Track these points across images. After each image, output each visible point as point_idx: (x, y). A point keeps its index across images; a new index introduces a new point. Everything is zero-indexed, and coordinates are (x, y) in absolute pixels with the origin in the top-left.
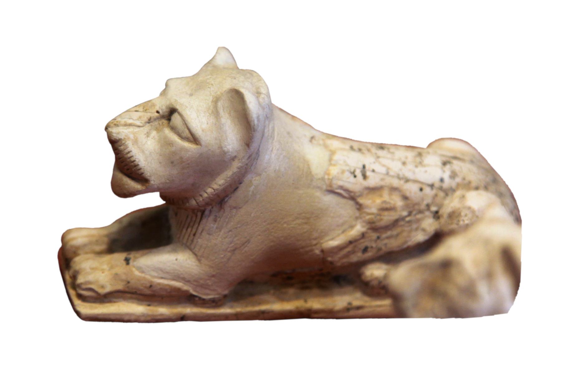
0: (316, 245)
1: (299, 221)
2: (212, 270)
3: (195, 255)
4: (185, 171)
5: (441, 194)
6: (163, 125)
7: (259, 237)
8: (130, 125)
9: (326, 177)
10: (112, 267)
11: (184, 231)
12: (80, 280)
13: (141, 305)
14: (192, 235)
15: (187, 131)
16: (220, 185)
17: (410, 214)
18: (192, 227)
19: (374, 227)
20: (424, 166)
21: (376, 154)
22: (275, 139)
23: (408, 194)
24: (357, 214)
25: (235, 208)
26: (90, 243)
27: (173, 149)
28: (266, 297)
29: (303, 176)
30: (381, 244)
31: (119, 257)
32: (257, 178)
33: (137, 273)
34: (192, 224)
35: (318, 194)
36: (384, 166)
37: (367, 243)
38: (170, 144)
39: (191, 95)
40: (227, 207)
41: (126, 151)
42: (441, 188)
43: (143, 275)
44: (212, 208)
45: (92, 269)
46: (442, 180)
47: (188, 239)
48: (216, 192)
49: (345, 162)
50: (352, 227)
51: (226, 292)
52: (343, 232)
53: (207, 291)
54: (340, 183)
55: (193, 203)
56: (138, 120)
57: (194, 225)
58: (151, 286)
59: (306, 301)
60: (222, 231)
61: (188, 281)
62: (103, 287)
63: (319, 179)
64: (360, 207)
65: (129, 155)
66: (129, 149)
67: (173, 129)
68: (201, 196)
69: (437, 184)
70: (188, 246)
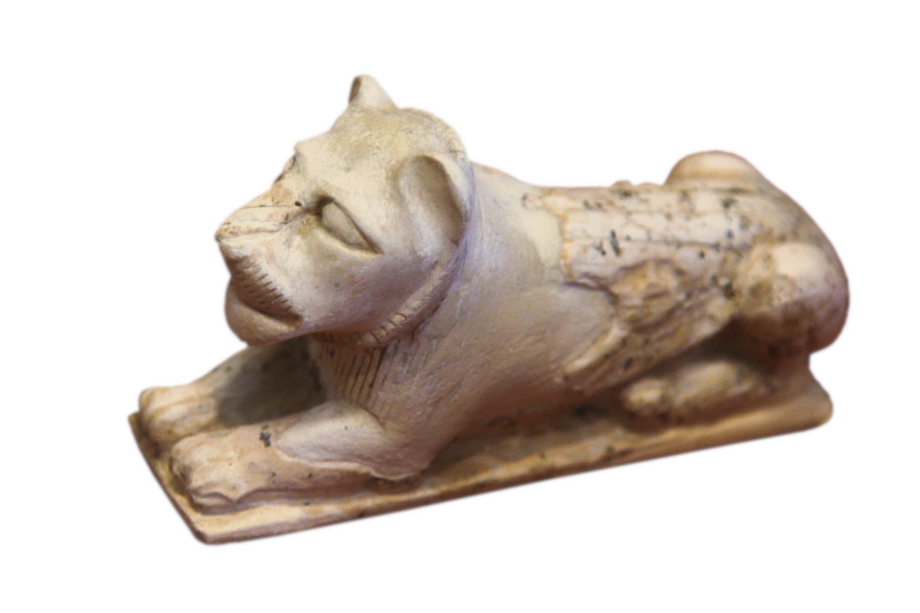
0: (555, 371)
1: (529, 340)
2: (403, 436)
3: (375, 416)
4: (360, 295)
5: (732, 257)
6: (310, 224)
7: (475, 376)
8: (257, 231)
9: (562, 262)
10: (242, 454)
11: (351, 380)
12: (197, 481)
13: (295, 505)
14: (366, 387)
15: (357, 234)
16: (414, 309)
17: (689, 296)
18: (366, 374)
19: (639, 327)
20: (699, 215)
21: (624, 207)
22: (484, 216)
23: (684, 267)
24: (611, 310)
25: (435, 338)
26: (191, 413)
27: (337, 264)
28: (479, 459)
29: (531, 270)
30: (651, 351)
31: (248, 434)
32: (466, 286)
33: (286, 458)
34: (364, 369)
35: (553, 291)
36: (641, 227)
37: (630, 353)
38: (331, 256)
39: (348, 170)
40: (422, 339)
41: (258, 275)
42: (730, 248)
43: (296, 460)
44: (399, 342)
45: (212, 460)
46: (730, 235)
47: (360, 392)
48: (409, 319)
49: (584, 232)
50: (605, 332)
51: (425, 465)
52: (594, 342)
53: (397, 469)
54: (584, 268)
55: (370, 339)
56: (268, 220)
57: (368, 370)
58: (310, 476)
59: (542, 456)
60: (418, 376)
61: (368, 459)
62: (234, 488)
63: (553, 268)
64: (614, 299)
65: (264, 281)
66: (263, 272)
67: (331, 230)
68: (383, 328)
69: (724, 243)
70: (363, 404)
